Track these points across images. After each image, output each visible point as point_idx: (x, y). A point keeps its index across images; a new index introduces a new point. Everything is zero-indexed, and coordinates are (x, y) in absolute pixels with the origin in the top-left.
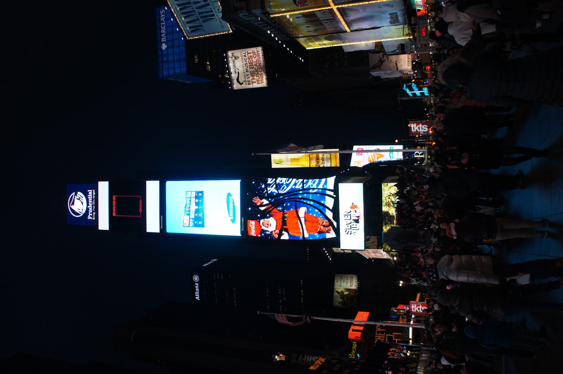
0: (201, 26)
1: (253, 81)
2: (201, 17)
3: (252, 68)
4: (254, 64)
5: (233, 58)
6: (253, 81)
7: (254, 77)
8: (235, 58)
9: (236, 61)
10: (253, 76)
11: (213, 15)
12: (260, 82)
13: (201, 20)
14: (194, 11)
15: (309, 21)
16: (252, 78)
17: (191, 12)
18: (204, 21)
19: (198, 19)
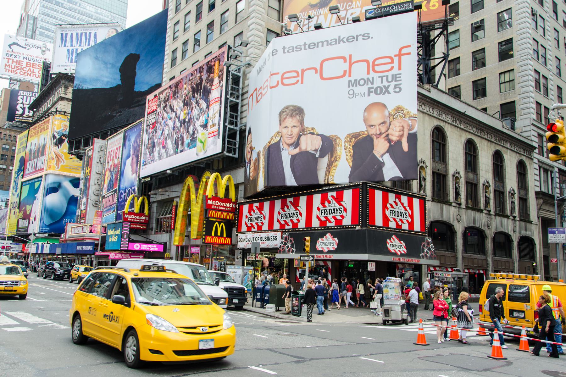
0: (65, 46)
1: (11, 61)
2: (73, 49)
3: (27, 64)
4: (32, 69)
5: (44, 49)
6: (11, 61)
7: (15, 64)
8: (44, 51)
9: (39, 51)
11: (71, 62)
12: (7, 68)
13: (71, 48)
14: (80, 46)
15: (39, 148)
16: (15, 60)
17: (81, 42)
18: (68, 50)
19: (72, 46)
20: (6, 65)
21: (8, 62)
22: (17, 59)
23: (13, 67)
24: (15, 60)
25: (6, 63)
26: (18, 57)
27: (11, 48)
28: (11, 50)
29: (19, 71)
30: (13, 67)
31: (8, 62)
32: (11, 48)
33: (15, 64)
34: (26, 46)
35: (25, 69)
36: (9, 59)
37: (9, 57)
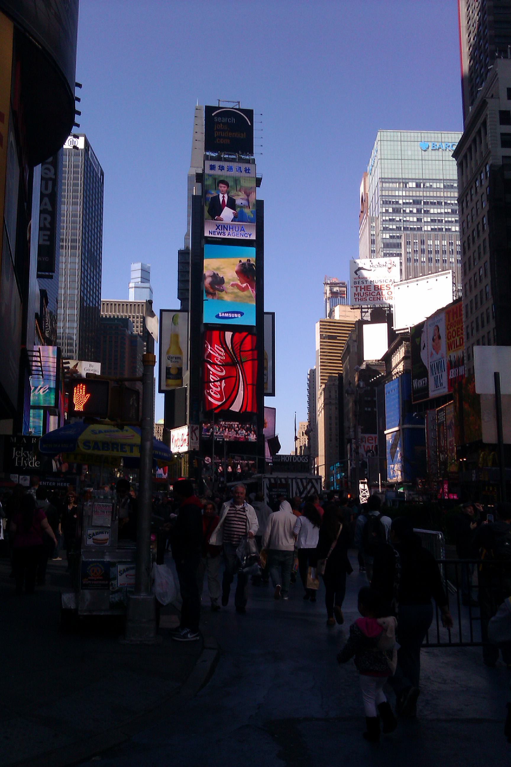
1: (359, 289)
6: (359, 289)
7: (363, 290)
10: (364, 288)
16: (363, 287)
20: (355, 293)
21: (357, 291)
22: (365, 284)
23: (362, 295)
24: (363, 287)
25: (355, 291)
26: (365, 282)
27: (357, 274)
28: (357, 276)
29: (369, 297)
30: (362, 295)
31: (357, 291)
32: (357, 274)
33: (363, 290)
34: (372, 268)
35: (373, 294)
36: (357, 287)
37: (357, 285)
